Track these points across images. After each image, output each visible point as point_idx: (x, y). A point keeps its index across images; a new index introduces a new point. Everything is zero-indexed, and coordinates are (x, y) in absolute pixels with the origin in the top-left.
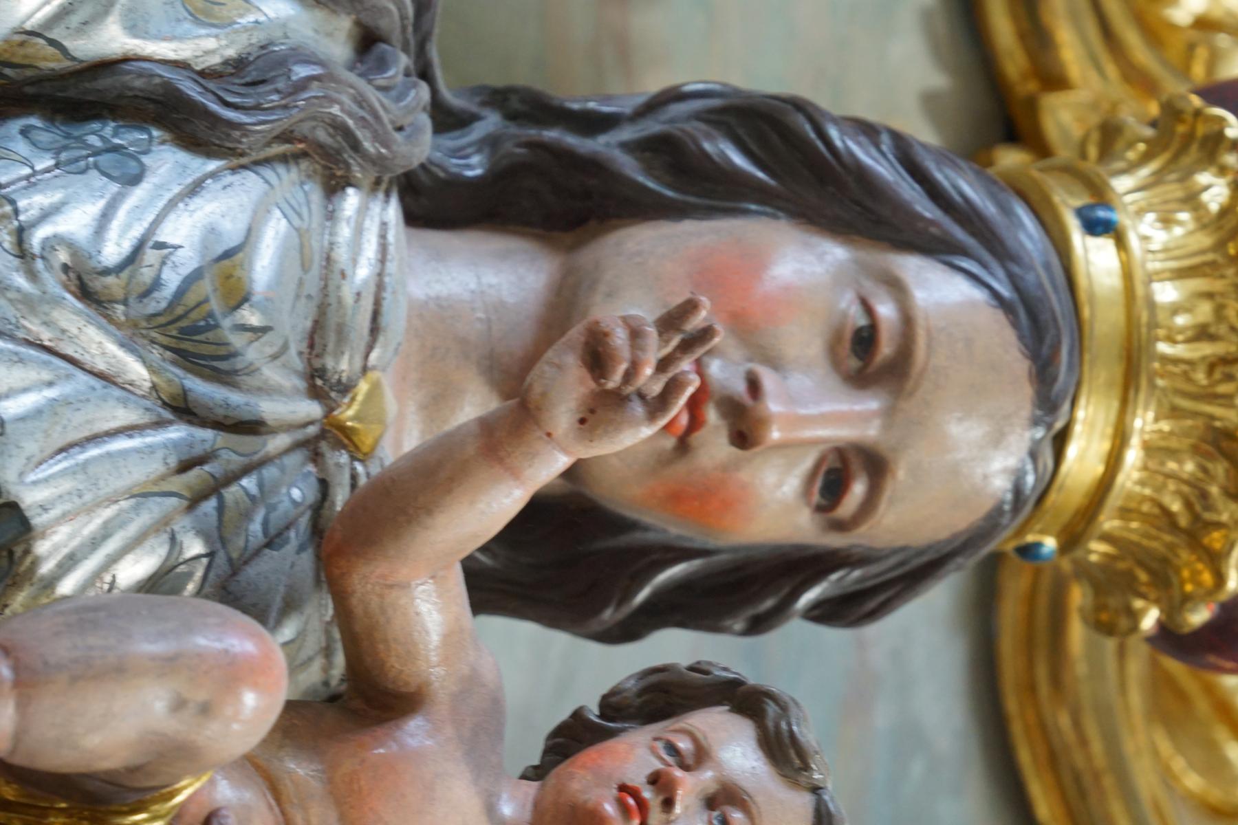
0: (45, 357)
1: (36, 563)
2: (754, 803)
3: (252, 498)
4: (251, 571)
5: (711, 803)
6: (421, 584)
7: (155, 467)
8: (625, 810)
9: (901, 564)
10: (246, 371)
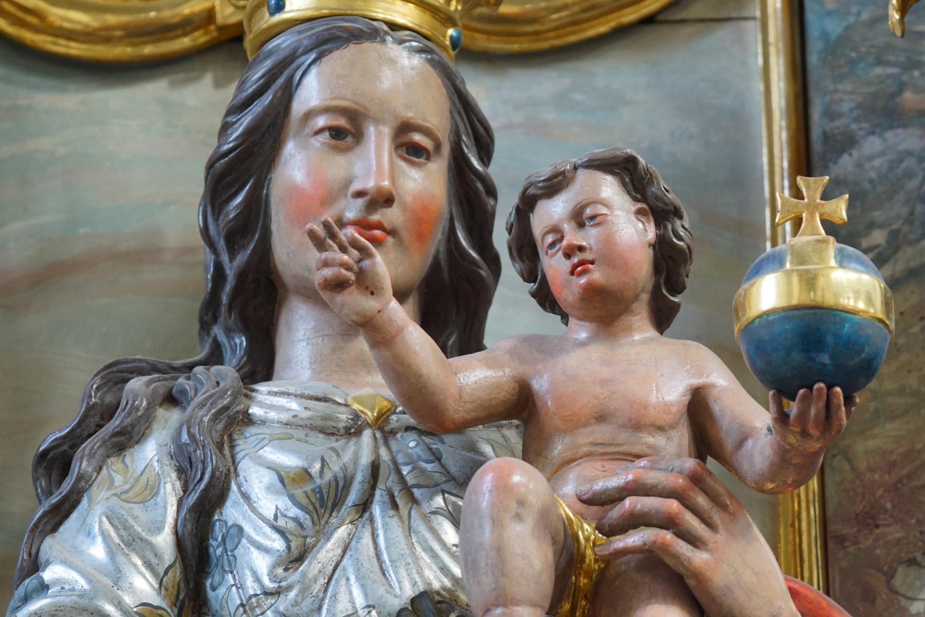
0: (333, 582)
1: (444, 588)
2: (582, 202)
3: (413, 469)
4: (453, 470)
5: (581, 225)
6: (460, 380)
7: (394, 522)
8: (584, 272)
9: (459, 113)
10: (345, 471)
